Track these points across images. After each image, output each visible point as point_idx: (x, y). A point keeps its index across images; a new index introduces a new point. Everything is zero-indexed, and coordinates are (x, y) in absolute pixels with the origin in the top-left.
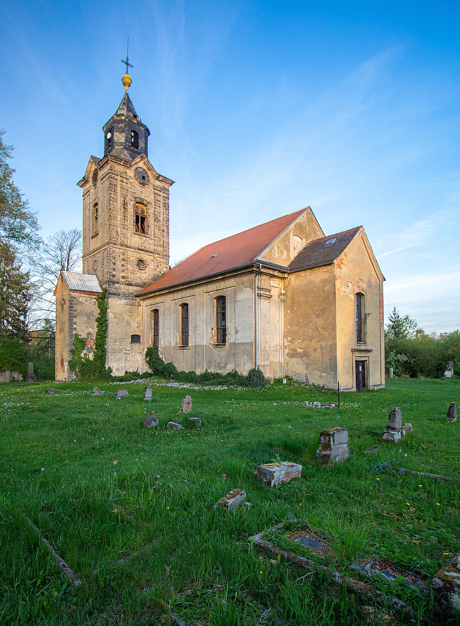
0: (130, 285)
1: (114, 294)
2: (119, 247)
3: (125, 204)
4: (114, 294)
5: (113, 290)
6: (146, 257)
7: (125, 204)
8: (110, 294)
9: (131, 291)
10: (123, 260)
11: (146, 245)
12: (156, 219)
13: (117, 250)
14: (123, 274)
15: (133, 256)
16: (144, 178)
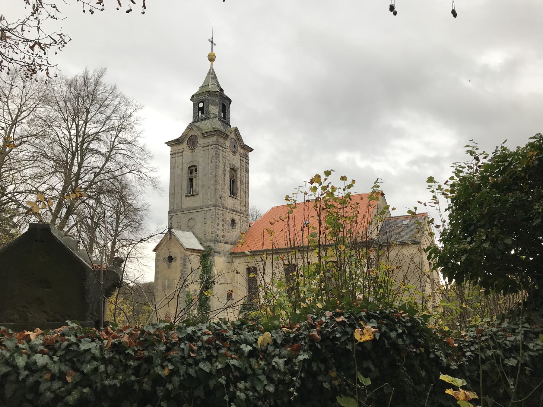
0: (227, 243)
1: (218, 252)
2: (220, 209)
3: (224, 171)
4: (218, 252)
5: (217, 249)
6: (236, 218)
7: (224, 171)
8: (215, 252)
9: (227, 249)
10: (223, 220)
11: (236, 206)
12: (242, 183)
13: (220, 212)
14: (223, 234)
15: (229, 216)
16: (235, 147)
